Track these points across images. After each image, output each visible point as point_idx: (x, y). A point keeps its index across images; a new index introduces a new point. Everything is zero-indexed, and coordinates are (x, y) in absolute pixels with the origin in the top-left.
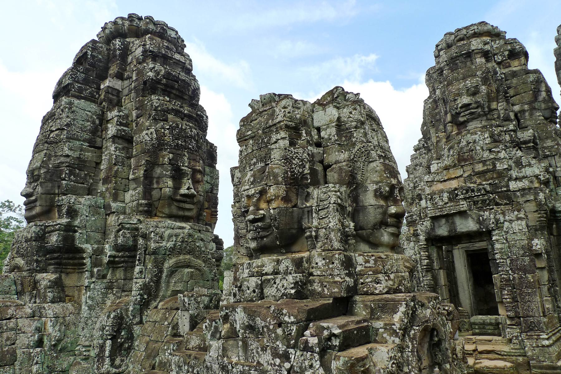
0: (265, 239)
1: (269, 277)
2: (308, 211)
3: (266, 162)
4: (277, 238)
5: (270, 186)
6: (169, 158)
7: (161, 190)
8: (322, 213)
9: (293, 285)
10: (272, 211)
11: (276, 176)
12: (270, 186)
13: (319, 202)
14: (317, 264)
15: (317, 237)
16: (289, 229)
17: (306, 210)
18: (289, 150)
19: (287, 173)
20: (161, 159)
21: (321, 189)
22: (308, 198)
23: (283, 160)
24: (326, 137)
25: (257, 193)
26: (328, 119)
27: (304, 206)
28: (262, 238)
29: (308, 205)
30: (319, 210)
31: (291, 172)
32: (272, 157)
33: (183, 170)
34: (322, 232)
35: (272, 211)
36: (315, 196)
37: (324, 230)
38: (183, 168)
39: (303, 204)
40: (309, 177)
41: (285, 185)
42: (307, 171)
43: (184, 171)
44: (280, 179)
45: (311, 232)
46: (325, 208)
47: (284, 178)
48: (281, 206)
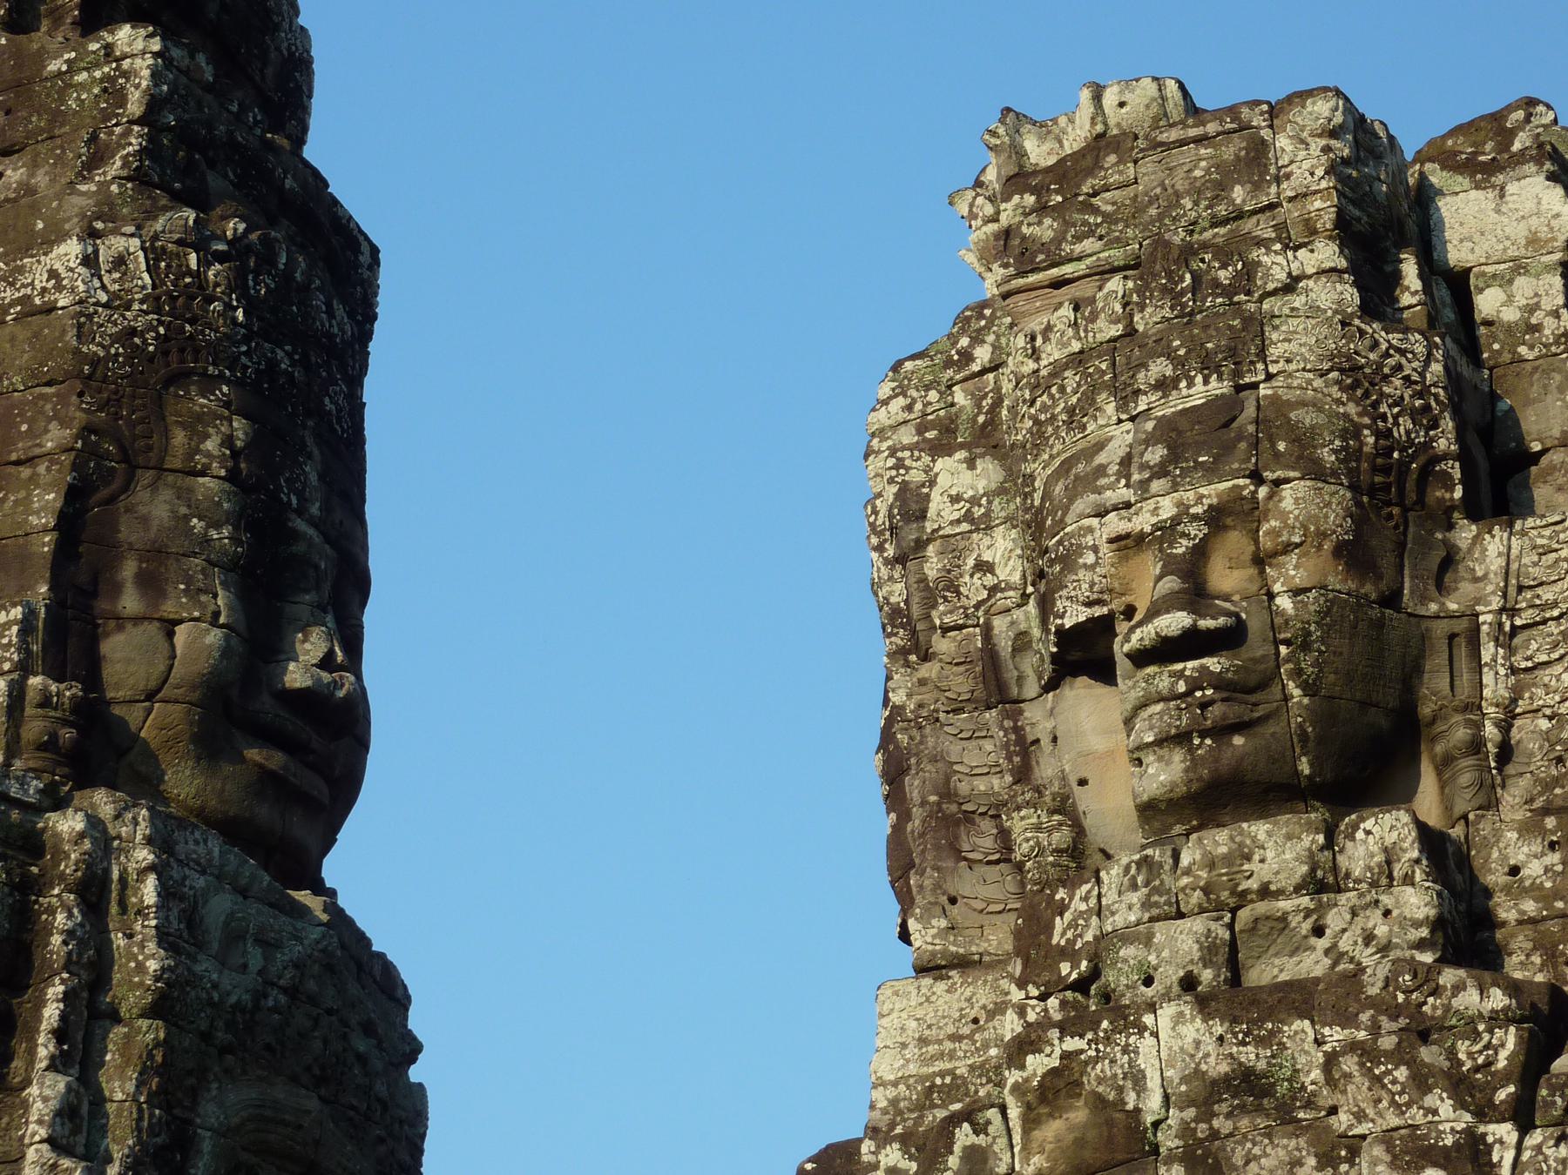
0: (1238, 740)
1: (1284, 905)
2: (1452, 637)
3: (1237, 374)
4: (1304, 737)
5: (1278, 483)
6: (228, 441)
7: (170, 635)
8: (1535, 647)
9: (1424, 932)
10: (1284, 603)
11: (1303, 441)
12: (1278, 483)
13: (1512, 591)
14: (1514, 871)
15: (1506, 752)
16: (1365, 705)
17: (1441, 629)
18: (1362, 333)
19: (1357, 435)
20: (179, 438)
21: (1523, 533)
22: (1448, 578)
23: (1334, 375)
24: (1510, 315)
25: (1195, 518)
26: (1520, 232)
27: (1433, 607)
28: (1222, 732)
29: (1453, 606)
30: (1515, 630)
31: (1378, 434)
32: (1274, 352)
33: (295, 535)
34: (1529, 732)
35: (1284, 603)
36: (1496, 564)
37: (1544, 724)
38: (300, 525)
39: (1424, 599)
40: (1457, 474)
41: (1351, 487)
42: (1444, 443)
43: (299, 548)
44: (1328, 457)
45: (1479, 726)
46: (1544, 622)
47: (1350, 456)
48: (1334, 582)
